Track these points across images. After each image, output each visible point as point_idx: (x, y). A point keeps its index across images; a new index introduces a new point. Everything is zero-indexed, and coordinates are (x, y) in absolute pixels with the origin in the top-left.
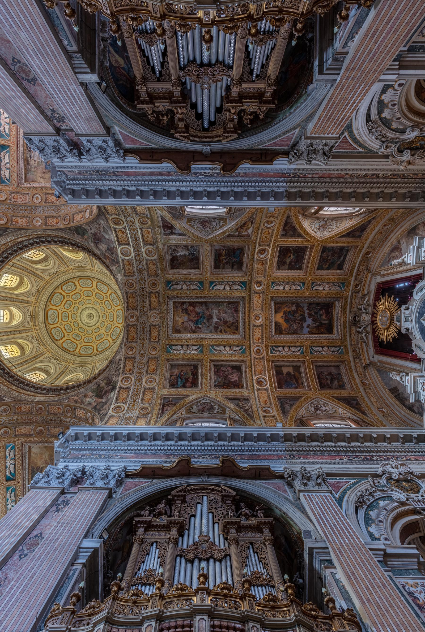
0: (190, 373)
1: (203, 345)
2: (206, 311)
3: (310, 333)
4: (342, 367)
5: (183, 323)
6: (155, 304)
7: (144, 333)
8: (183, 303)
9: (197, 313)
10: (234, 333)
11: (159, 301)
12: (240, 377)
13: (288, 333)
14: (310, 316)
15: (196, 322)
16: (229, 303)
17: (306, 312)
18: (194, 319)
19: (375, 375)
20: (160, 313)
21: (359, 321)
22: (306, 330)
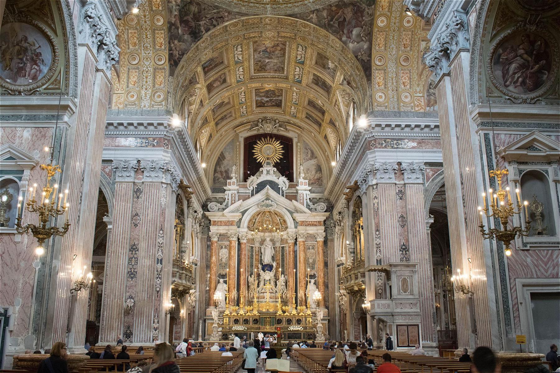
0: (217, 63)
1: (242, 63)
2: (276, 56)
3: (257, 101)
4: (232, 118)
5: (264, 44)
6: (283, 34)
7: (253, 28)
8: (284, 45)
9: (273, 52)
10: (255, 70)
11: (287, 37)
12: (217, 87)
13: (256, 92)
14: (271, 100)
15: (265, 51)
16: (283, 69)
17: (274, 99)
18: (268, 50)
19: (229, 137)
20: (274, 37)
21: (267, 122)
22: (259, 99)
